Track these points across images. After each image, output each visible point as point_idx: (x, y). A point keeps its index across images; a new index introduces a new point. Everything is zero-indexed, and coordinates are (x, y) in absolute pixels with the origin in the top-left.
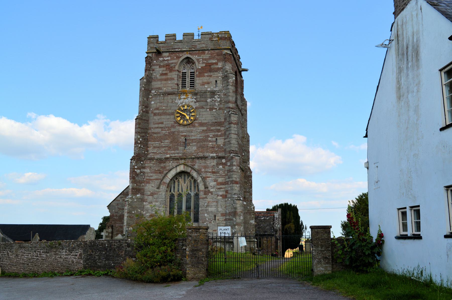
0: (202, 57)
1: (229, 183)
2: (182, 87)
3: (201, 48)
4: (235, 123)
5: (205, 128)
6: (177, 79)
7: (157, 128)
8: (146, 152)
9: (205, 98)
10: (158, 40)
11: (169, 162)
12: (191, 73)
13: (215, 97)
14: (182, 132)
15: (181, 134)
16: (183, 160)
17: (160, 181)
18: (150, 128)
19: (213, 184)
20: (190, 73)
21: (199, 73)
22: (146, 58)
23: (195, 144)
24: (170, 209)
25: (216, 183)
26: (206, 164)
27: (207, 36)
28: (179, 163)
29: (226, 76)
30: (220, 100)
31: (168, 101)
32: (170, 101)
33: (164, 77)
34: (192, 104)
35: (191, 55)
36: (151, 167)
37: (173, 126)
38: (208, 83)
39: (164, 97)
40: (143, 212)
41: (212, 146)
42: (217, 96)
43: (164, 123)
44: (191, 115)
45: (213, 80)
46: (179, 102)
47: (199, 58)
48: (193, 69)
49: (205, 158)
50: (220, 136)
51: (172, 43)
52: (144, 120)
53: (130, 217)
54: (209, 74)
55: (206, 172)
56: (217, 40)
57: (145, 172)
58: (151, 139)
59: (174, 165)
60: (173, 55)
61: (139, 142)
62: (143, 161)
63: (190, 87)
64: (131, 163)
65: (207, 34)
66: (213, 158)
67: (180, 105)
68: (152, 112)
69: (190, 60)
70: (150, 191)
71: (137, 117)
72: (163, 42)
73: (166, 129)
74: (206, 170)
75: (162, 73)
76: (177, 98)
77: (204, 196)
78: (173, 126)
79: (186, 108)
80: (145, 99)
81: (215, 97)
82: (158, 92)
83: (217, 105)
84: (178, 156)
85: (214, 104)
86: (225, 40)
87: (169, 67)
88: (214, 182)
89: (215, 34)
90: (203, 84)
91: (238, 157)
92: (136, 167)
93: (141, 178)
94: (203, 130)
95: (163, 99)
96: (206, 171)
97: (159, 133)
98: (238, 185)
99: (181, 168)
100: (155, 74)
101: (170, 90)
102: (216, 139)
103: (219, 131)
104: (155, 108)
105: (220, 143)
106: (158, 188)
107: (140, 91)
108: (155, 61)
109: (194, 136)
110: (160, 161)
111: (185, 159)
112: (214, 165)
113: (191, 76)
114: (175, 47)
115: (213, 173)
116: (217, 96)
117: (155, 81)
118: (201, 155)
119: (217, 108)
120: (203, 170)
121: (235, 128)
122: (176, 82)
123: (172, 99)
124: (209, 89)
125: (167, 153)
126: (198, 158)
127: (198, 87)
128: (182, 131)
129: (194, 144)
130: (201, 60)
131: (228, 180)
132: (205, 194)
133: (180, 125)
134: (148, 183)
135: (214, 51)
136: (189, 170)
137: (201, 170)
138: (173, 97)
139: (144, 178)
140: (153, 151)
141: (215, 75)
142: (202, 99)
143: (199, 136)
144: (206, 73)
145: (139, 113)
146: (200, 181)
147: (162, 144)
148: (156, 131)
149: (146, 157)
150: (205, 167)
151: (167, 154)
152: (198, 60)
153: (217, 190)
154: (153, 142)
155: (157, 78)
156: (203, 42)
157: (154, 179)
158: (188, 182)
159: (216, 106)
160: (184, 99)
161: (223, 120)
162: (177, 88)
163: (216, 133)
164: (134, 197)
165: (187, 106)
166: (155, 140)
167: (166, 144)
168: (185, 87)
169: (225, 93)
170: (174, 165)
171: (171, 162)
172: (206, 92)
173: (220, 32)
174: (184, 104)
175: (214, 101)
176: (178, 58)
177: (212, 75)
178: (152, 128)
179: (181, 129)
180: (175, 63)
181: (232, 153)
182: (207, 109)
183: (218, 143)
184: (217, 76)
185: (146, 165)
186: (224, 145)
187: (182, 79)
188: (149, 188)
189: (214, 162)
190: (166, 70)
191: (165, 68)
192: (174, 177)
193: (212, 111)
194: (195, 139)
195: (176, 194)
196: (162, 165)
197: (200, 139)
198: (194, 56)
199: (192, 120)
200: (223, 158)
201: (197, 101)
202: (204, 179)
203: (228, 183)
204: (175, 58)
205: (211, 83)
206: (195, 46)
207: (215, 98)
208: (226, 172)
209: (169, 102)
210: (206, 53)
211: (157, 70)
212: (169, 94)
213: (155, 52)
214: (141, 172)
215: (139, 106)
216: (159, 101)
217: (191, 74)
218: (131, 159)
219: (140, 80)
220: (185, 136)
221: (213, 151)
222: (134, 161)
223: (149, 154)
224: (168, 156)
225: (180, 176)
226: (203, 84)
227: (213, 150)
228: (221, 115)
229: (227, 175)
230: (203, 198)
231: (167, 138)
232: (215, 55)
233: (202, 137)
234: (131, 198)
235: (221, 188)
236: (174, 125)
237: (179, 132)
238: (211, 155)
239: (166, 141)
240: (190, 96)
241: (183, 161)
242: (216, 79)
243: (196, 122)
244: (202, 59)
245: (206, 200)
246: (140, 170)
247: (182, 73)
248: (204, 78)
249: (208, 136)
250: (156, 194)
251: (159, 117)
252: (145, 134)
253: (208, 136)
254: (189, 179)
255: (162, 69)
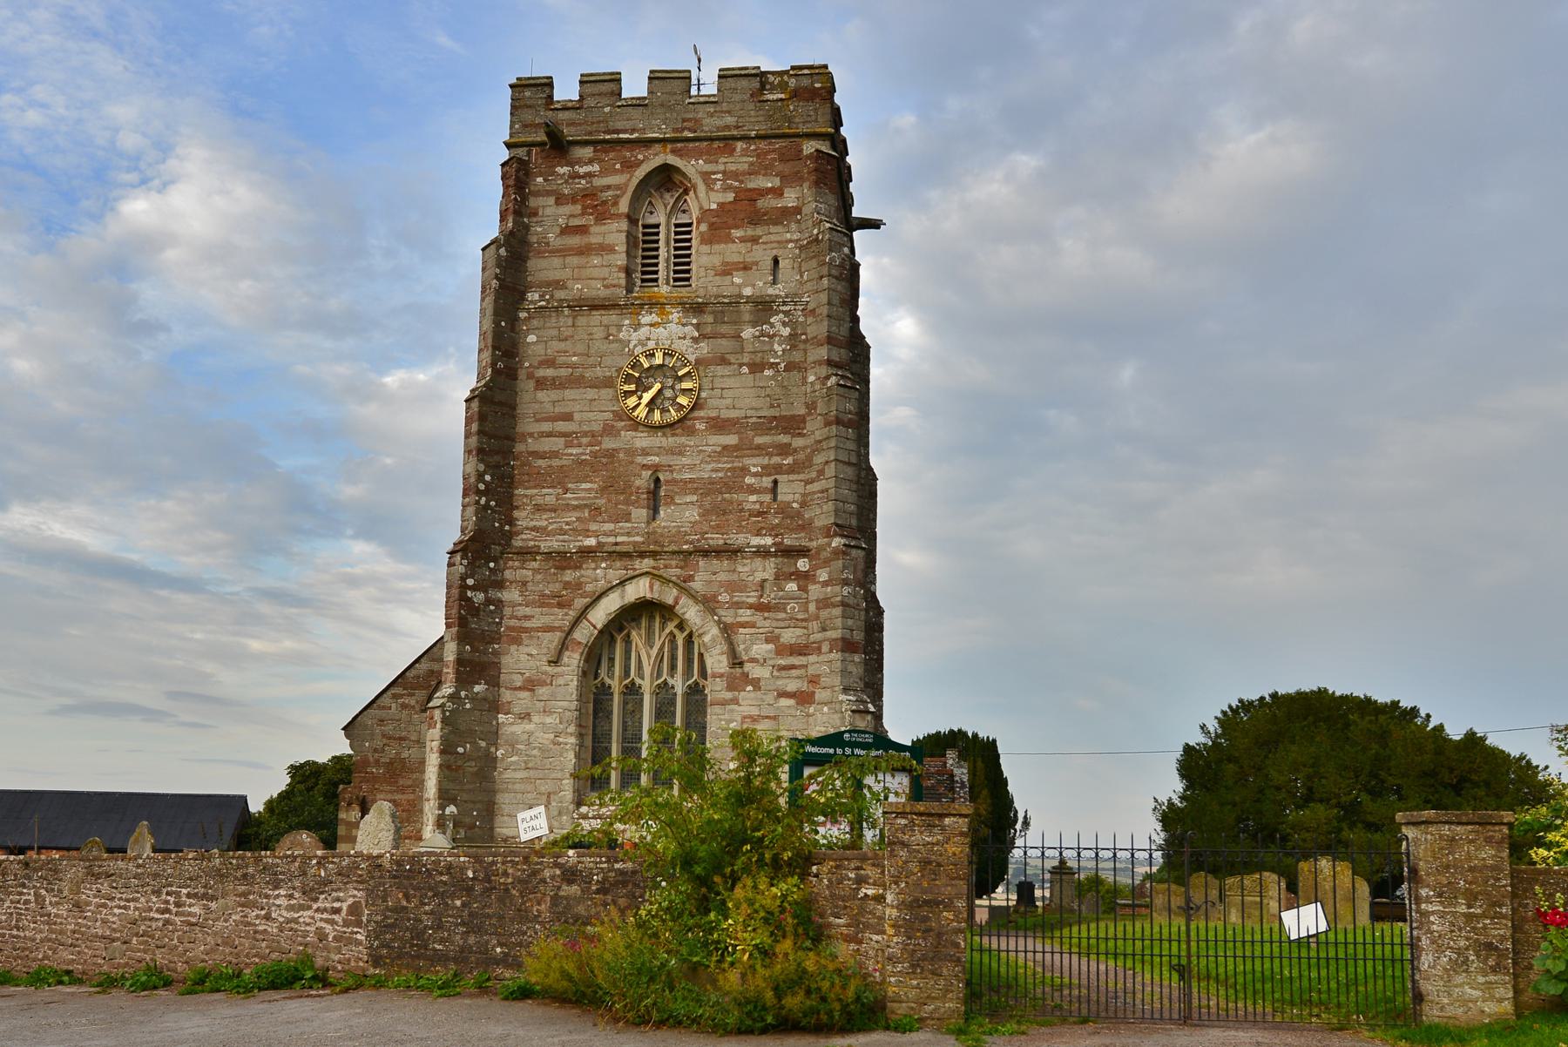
0: (721, 168)
1: (825, 648)
2: (643, 281)
3: (718, 129)
4: (850, 420)
5: (732, 440)
6: (624, 248)
7: (550, 435)
8: (507, 528)
9: (735, 323)
10: (551, 97)
11: (593, 565)
12: (677, 226)
13: (772, 320)
14: (645, 452)
15: (639, 459)
16: (646, 560)
17: (558, 635)
18: (524, 436)
19: (761, 649)
20: (673, 229)
21: (712, 226)
22: (503, 165)
23: (695, 498)
24: (594, 742)
25: (771, 646)
26: (735, 577)
27: (744, 83)
28: (635, 569)
29: (817, 240)
30: (790, 334)
31: (591, 334)
32: (599, 333)
33: (575, 241)
34: (682, 346)
35: (681, 156)
36: (524, 584)
37: (609, 430)
38: (746, 267)
39: (574, 318)
40: (497, 750)
41: (757, 506)
42: (781, 315)
43: (577, 416)
44: (678, 387)
45: (762, 255)
46: (635, 337)
47: (709, 168)
48: (684, 212)
49: (732, 552)
50: (791, 470)
51: (607, 110)
52: (501, 404)
53: (449, 767)
54: (750, 232)
55: (738, 605)
56: (781, 100)
57: (502, 602)
58: (526, 478)
59: (615, 575)
60: (612, 155)
61: (482, 487)
62: (495, 560)
63: (676, 280)
64: (450, 565)
65: (741, 75)
66: (763, 553)
67: (638, 350)
68: (530, 376)
69: (677, 178)
70: (522, 674)
71: (473, 391)
72: (570, 105)
73: (585, 440)
74: (735, 599)
75: (567, 226)
76: (627, 322)
77: (729, 695)
78: (609, 430)
79: (658, 360)
80: (503, 324)
81: (772, 320)
82: (552, 296)
83: (780, 353)
84: (629, 543)
85: (766, 348)
86: (812, 100)
87: (595, 204)
88: (767, 641)
89: (771, 78)
90: (726, 270)
91: (859, 551)
92: (470, 582)
93: (489, 624)
94: (725, 448)
95: (573, 326)
96: (737, 603)
97: (555, 455)
98: (857, 658)
99: (638, 590)
100: (539, 229)
101: (597, 290)
102: (775, 482)
103: (784, 450)
104: (539, 359)
105: (789, 498)
106: (555, 662)
107: (483, 292)
108: (540, 180)
109: (692, 467)
110: (562, 560)
111: (654, 555)
112: (765, 581)
113: (676, 241)
114: (619, 125)
115: (760, 608)
116: (781, 315)
117: (539, 254)
118: (716, 540)
119: (779, 363)
120: (724, 597)
121: (848, 442)
122: (621, 260)
123: (607, 327)
124: (748, 291)
125: (588, 530)
126: (706, 553)
127: (703, 280)
128: (643, 449)
129: (689, 499)
130: (719, 176)
131: (818, 636)
132: (730, 688)
133: (636, 425)
134: (517, 641)
135: (770, 144)
136: (669, 596)
137: (715, 596)
138: (611, 317)
139: (500, 623)
140: (532, 524)
141: (772, 238)
142: (724, 329)
143: (710, 467)
144: (737, 227)
145: (480, 376)
146: (713, 640)
147: (568, 495)
148: (547, 449)
149: (509, 544)
150: (732, 587)
151: (587, 533)
152: (706, 176)
153: (775, 673)
154: (535, 487)
155: (547, 244)
156: (725, 106)
157: (538, 630)
158: (664, 643)
159: (777, 357)
160: (651, 325)
161: (803, 411)
162: (623, 282)
163: (776, 460)
164: (463, 694)
165: (664, 354)
166: (541, 479)
167: (584, 499)
168: (656, 280)
169: (810, 307)
170: (615, 575)
171: (604, 565)
172: (736, 301)
173: (793, 68)
174: (651, 345)
175: (769, 336)
176: (630, 166)
177: (760, 237)
178: (531, 435)
179: (642, 440)
180: (618, 187)
181: (836, 535)
182: (741, 365)
183: (779, 498)
184: (778, 238)
185: (508, 574)
186: (803, 504)
187: (644, 250)
188: (520, 660)
189: (765, 570)
190: (583, 214)
191: (579, 207)
192: (611, 622)
193: (758, 375)
194: (692, 481)
195: (616, 685)
196: (569, 576)
197: (712, 482)
198: (693, 162)
199: (682, 406)
200: (802, 552)
201: (703, 337)
202: (727, 630)
203: (819, 649)
204: (618, 166)
205: (755, 268)
206: (696, 121)
207: (772, 326)
208: (812, 607)
209: (595, 336)
210: (738, 149)
211: (548, 211)
212: (596, 306)
213: (542, 144)
214: (488, 601)
215: (480, 351)
216: (554, 332)
217: (677, 233)
218: (452, 553)
219: (483, 249)
220: (656, 468)
221: (762, 528)
222: (462, 559)
223: (518, 533)
224: (591, 542)
225: (633, 620)
226: (726, 270)
227: (763, 525)
228: (795, 390)
229: (817, 618)
230: (723, 703)
231: (588, 476)
232: (775, 159)
233: (720, 475)
234: (451, 697)
235: (793, 667)
236: (613, 426)
237: (631, 452)
238: (756, 541)
239: (584, 486)
240: (675, 315)
241: (646, 564)
242: (775, 252)
243: (697, 414)
244: (724, 172)
245: (732, 711)
246: (486, 592)
247: (645, 226)
248: (730, 245)
249: (745, 471)
250: (543, 684)
251: (554, 395)
252: (504, 458)
253: (745, 471)
254: (667, 631)
255: (568, 209)
